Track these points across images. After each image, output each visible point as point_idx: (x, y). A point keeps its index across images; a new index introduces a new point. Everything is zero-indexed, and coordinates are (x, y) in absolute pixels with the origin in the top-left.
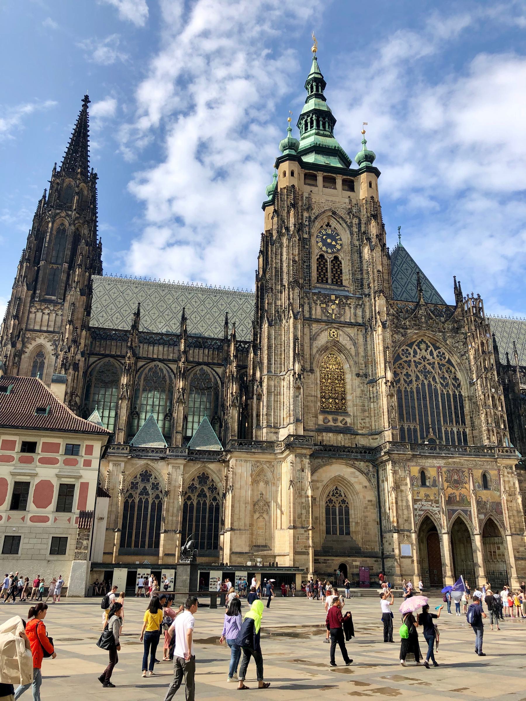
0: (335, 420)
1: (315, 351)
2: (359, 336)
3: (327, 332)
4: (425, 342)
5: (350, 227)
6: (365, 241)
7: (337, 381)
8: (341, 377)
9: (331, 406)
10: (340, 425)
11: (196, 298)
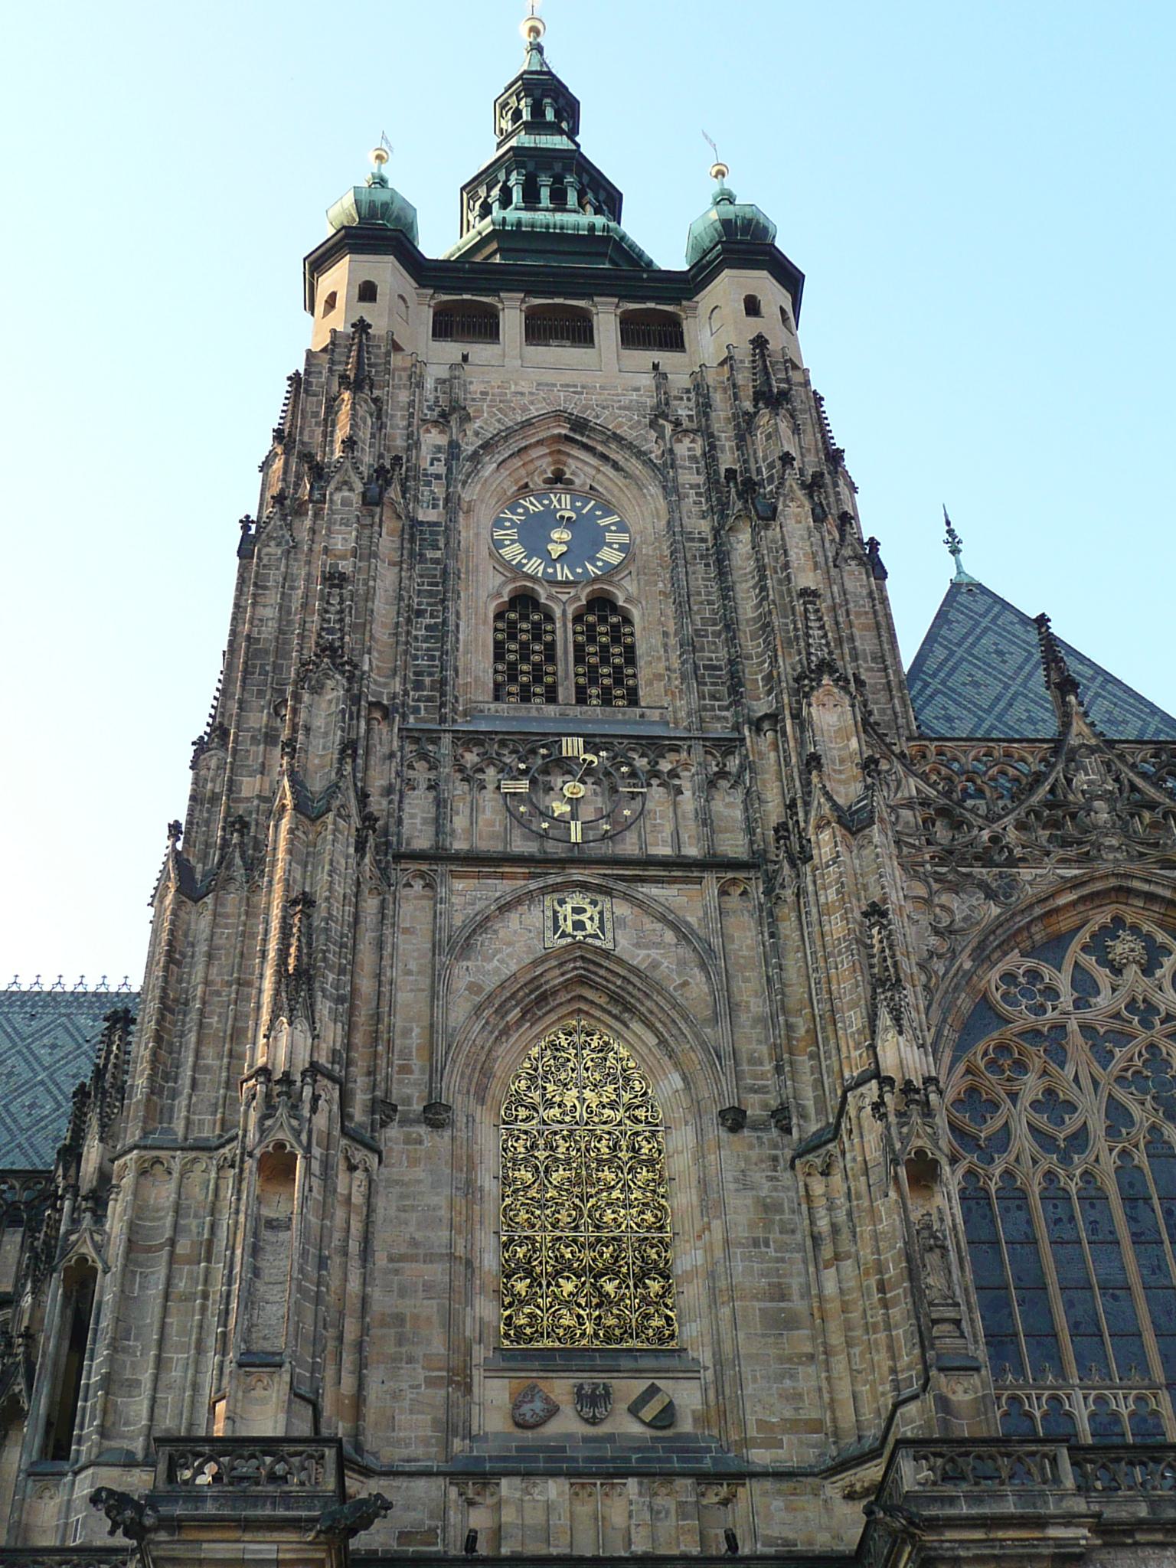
0: (593, 1401)
1: (459, 1012)
2: (731, 921)
3: (536, 911)
4: (1135, 929)
5: (664, 469)
6: (739, 505)
7: (608, 1175)
8: (634, 1150)
9: (564, 1322)
10: (636, 1428)
11: (60, 1032)
